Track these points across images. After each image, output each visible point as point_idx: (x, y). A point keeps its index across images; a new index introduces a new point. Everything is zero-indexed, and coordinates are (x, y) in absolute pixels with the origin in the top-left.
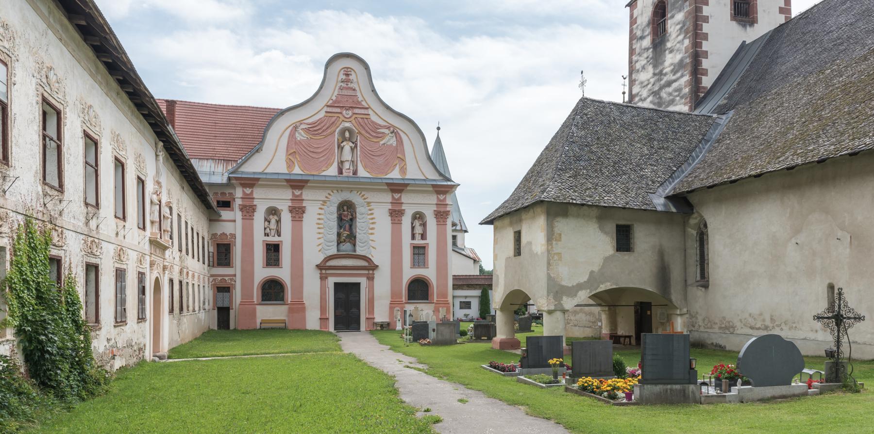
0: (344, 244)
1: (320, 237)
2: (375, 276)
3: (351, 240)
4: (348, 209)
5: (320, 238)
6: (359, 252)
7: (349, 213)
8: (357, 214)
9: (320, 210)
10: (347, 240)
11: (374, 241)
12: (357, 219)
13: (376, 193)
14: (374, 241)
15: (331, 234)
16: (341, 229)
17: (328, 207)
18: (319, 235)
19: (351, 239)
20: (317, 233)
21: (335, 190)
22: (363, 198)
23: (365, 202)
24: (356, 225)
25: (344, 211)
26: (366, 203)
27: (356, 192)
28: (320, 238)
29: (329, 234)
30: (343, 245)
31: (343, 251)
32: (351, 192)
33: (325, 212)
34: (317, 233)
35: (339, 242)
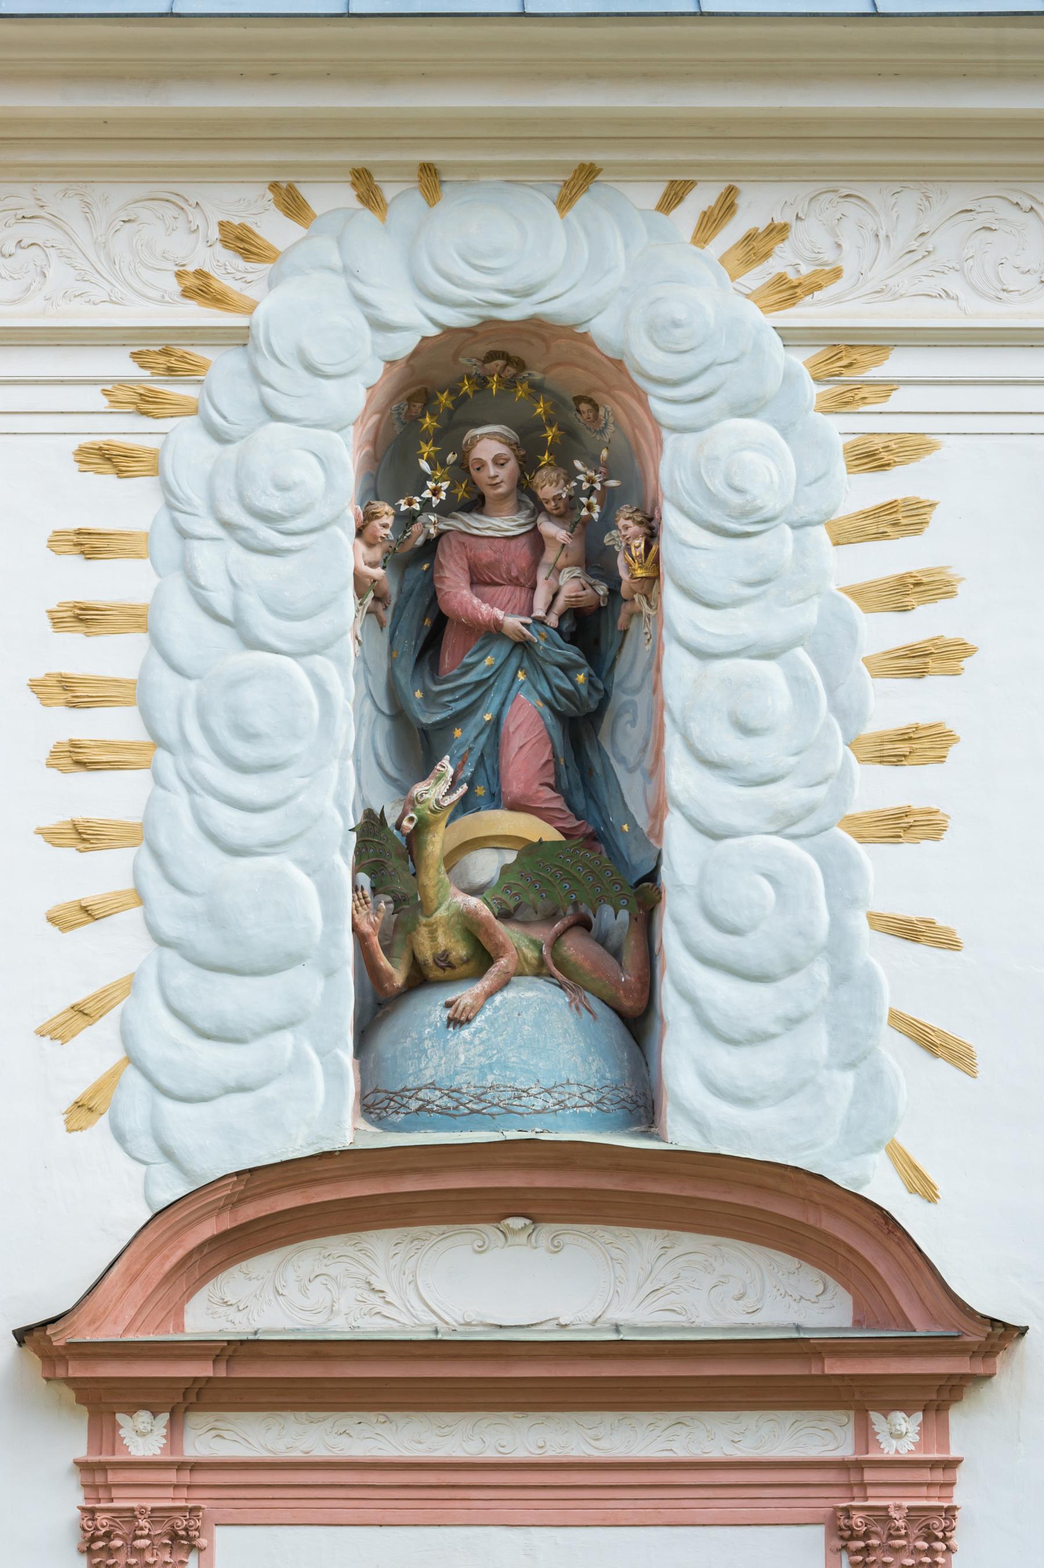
0: (466, 994)
1: (88, 893)
2: (959, 1497)
3: (575, 948)
4: (528, 465)
5: (88, 912)
6: (701, 1126)
7: (549, 528)
8: (671, 519)
9: (106, 482)
10: (509, 934)
11: (947, 942)
12: (671, 599)
13: (959, 196)
14: (947, 942)
15: (271, 847)
16: (425, 768)
17: (221, 438)
18: (69, 855)
19: (584, 924)
20: (52, 836)
21: (324, 172)
22: (757, 277)
23: (790, 337)
24: (658, 706)
25: (477, 504)
26: (799, 359)
27: (654, 192)
28: (88, 912)
29: (235, 851)
30: (456, 1022)
31: (449, 1116)
32: (564, 203)
33: (172, 502)
34: (52, 836)
35: (399, 978)
